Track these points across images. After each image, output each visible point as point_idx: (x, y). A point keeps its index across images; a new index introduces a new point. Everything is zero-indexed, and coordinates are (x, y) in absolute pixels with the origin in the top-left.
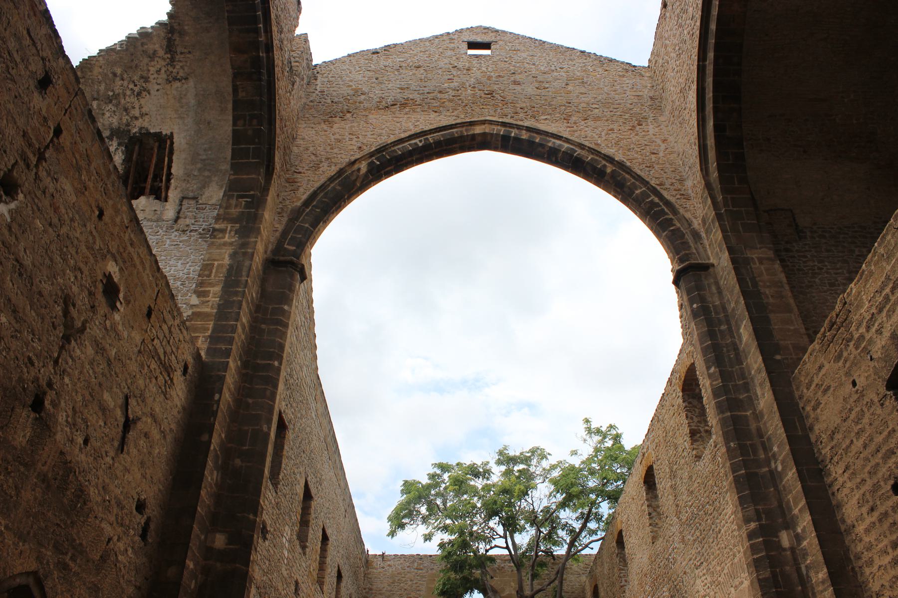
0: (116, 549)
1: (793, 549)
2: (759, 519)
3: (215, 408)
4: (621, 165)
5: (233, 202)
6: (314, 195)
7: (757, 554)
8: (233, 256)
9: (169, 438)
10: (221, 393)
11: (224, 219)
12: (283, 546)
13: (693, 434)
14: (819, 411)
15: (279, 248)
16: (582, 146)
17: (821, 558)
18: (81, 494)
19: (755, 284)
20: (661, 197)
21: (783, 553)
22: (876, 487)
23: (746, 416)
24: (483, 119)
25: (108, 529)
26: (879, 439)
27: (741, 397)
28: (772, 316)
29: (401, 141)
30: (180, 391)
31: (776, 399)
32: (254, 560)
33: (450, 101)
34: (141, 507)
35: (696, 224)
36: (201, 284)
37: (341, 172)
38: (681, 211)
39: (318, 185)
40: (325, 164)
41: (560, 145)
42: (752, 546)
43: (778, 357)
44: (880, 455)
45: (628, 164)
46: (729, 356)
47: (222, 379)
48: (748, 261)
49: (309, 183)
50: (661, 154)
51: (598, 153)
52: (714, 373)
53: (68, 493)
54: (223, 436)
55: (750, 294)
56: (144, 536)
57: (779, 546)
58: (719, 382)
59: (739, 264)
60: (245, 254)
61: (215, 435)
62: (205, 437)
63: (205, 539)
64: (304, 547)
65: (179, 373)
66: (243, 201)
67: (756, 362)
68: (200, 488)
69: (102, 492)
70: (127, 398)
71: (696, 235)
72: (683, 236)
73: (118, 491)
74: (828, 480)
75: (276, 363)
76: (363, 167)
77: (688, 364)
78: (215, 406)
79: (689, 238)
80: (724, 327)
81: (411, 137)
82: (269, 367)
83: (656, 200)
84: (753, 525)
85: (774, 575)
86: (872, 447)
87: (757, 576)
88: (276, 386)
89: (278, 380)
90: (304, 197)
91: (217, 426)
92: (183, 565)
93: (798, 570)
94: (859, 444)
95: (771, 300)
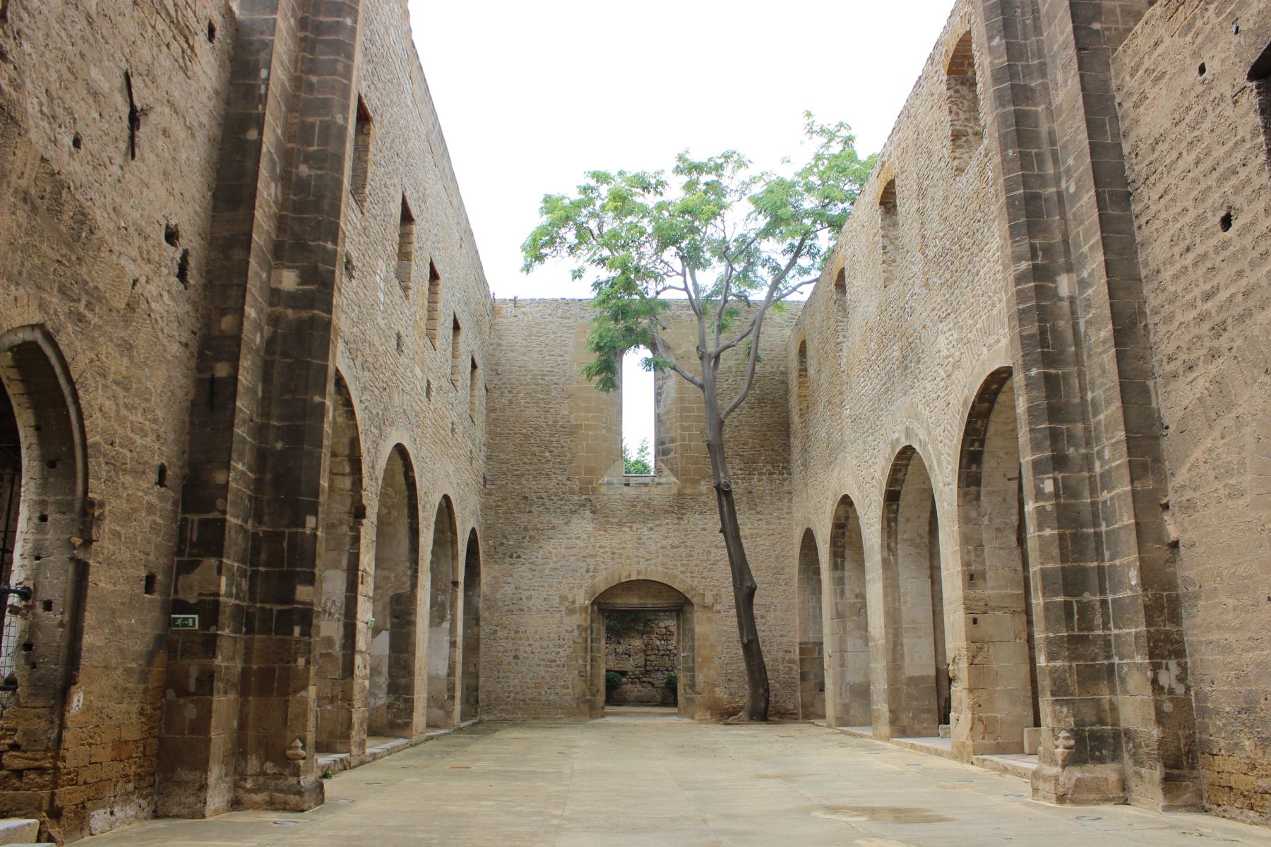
0: (146, 294)
1: (1072, 300)
2: (1034, 256)
3: (263, 91)
7: (1024, 302)
9: (201, 136)
10: (269, 69)
12: (376, 287)
13: (956, 136)
14: (1142, 109)
17: (1107, 312)
18: (82, 217)
21: (1059, 304)
22: (1201, 218)
23: (1036, 113)
25: (132, 270)
26: (1219, 152)
27: (1033, 84)
30: (208, 67)
31: (1083, 89)
32: (338, 305)
34: (172, 236)
42: (1019, 293)
43: (1096, 26)
44: (1215, 175)
46: (1024, 21)
47: (268, 46)
52: (999, 46)
53: (65, 217)
54: (279, 132)
56: (182, 275)
58: (1003, 60)
61: (267, 131)
62: (252, 135)
63: (267, 278)
64: (406, 289)
65: (202, 37)
67: (1062, 33)
68: (253, 208)
69: (113, 215)
70: (127, 77)
73: (136, 215)
74: (1136, 208)
75: (349, 21)
77: (962, 32)
78: (263, 88)
82: (337, 27)
84: (1024, 265)
85: (1043, 332)
86: (1207, 164)
87: (1021, 332)
88: (350, 56)
89: (353, 47)
91: (269, 118)
92: (240, 312)
93: (1075, 326)
94: (1189, 159)
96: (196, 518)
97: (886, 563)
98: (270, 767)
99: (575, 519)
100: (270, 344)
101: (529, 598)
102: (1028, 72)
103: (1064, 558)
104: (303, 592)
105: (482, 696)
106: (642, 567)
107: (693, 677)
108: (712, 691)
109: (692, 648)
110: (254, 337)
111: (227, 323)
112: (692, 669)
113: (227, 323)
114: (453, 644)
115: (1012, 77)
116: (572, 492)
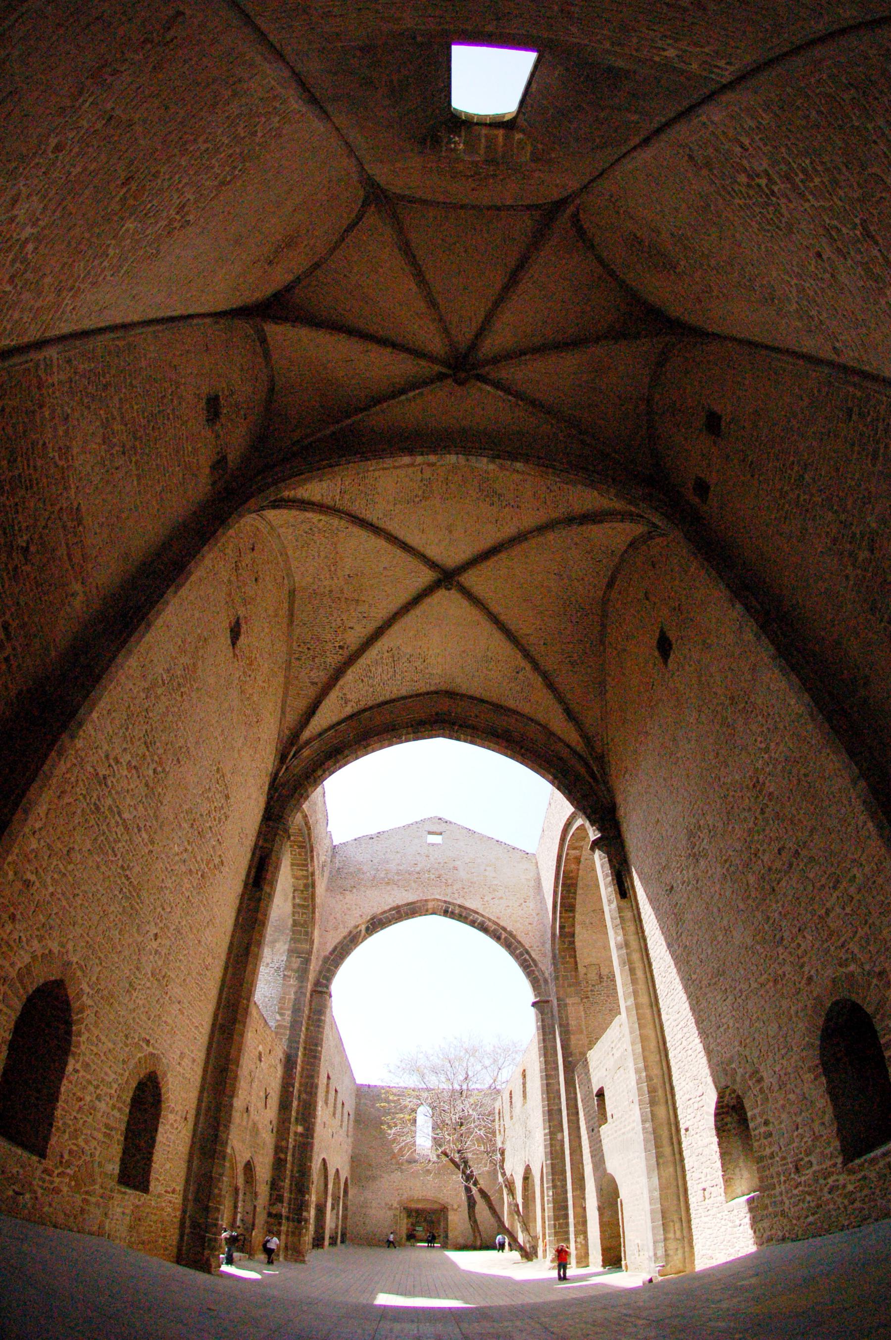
4: (510, 933)
5: (294, 959)
6: (335, 948)
8: (296, 993)
15: (317, 983)
16: (489, 920)
19: (567, 1019)
20: (530, 956)
24: (433, 897)
28: (572, 1036)
29: (384, 912)
33: (415, 882)
35: (547, 975)
36: (281, 1008)
37: (351, 932)
39: (337, 941)
40: (341, 926)
41: (477, 919)
45: (515, 933)
47: (296, 1063)
48: (566, 1005)
49: (333, 939)
50: (535, 924)
51: (498, 925)
66: (299, 960)
71: (546, 981)
76: (363, 927)
79: (541, 981)
81: (391, 910)
83: (528, 958)
90: (330, 949)
100: (294, 1147)
110: (291, 1146)
111: (284, 1143)
113: (284, 1143)
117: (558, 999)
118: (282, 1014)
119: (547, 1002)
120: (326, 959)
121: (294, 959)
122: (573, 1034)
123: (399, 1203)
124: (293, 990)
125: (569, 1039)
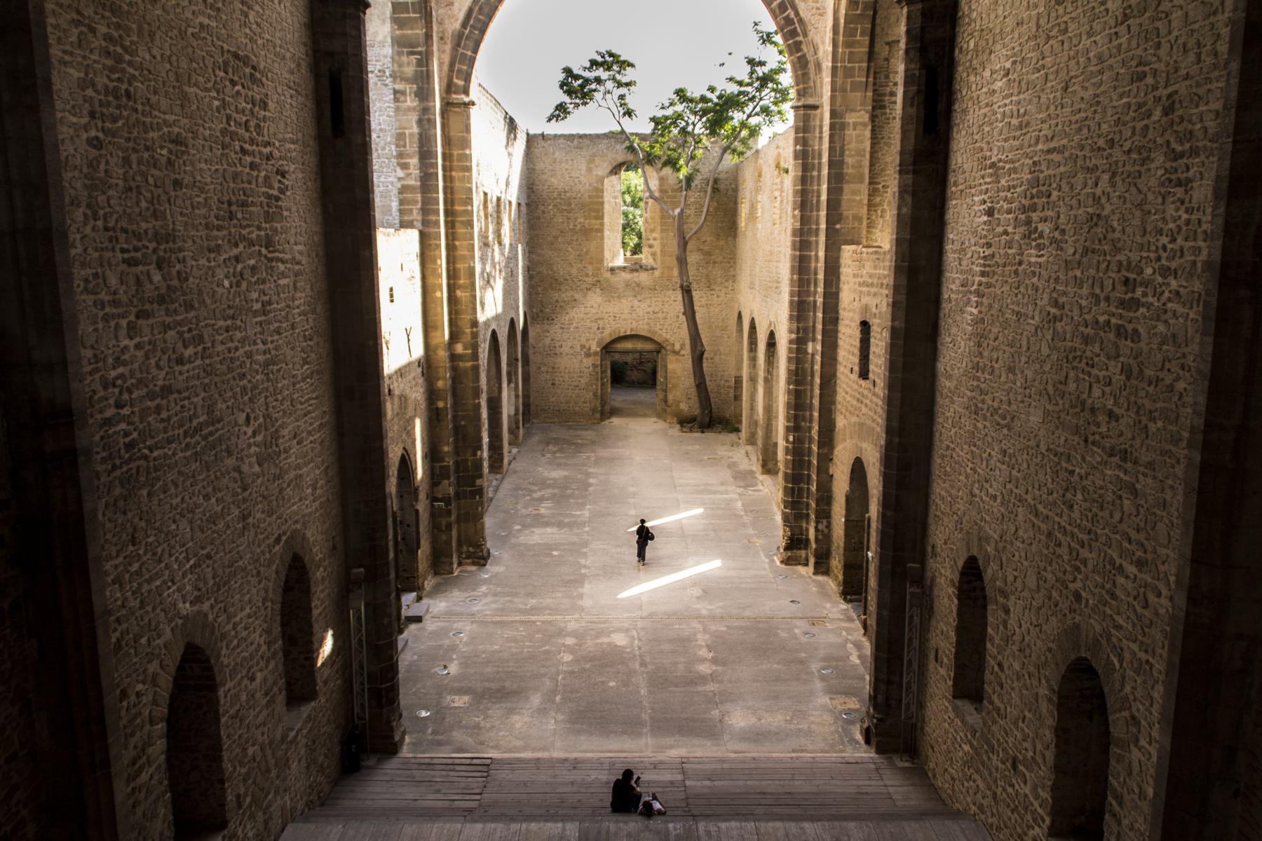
8: (420, 122)
11: (402, 79)
19: (842, 154)
36: (400, 155)
38: (811, 35)
43: (838, 226)
55: (836, 164)
57: (806, 352)
58: (798, 225)
59: (837, 127)
60: (429, 120)
62: (438, 294)
66: (413, 58)
71: (818, 66)
72: (807, 63)
80: (815, 173)
84: (794, 336)
85: (797, 369)
90: (461, 15)
95: (850, 171)
96: (438, 465)
97: (766, 380)
98: (471, 549)
99: (590, 294)
101: (561, 346)
102: (810, 232)
103: (793, 469)
104: (478, 482)
105: (532, 408)
106: (634, 325)
107: (666, 396)
108: (678, 405)
109: (666, 378)
112: (665, 391)
114: (517, 396)
115: (801, 235)
116: (587, 275)
117: (833, 114)
118: (404, 166)
119: (815, 107)
120: (459, 38)
121: (405, 59)
122: (848, 182)
123: (598, 344)
124: (414, 117)
125: (840, 190)
